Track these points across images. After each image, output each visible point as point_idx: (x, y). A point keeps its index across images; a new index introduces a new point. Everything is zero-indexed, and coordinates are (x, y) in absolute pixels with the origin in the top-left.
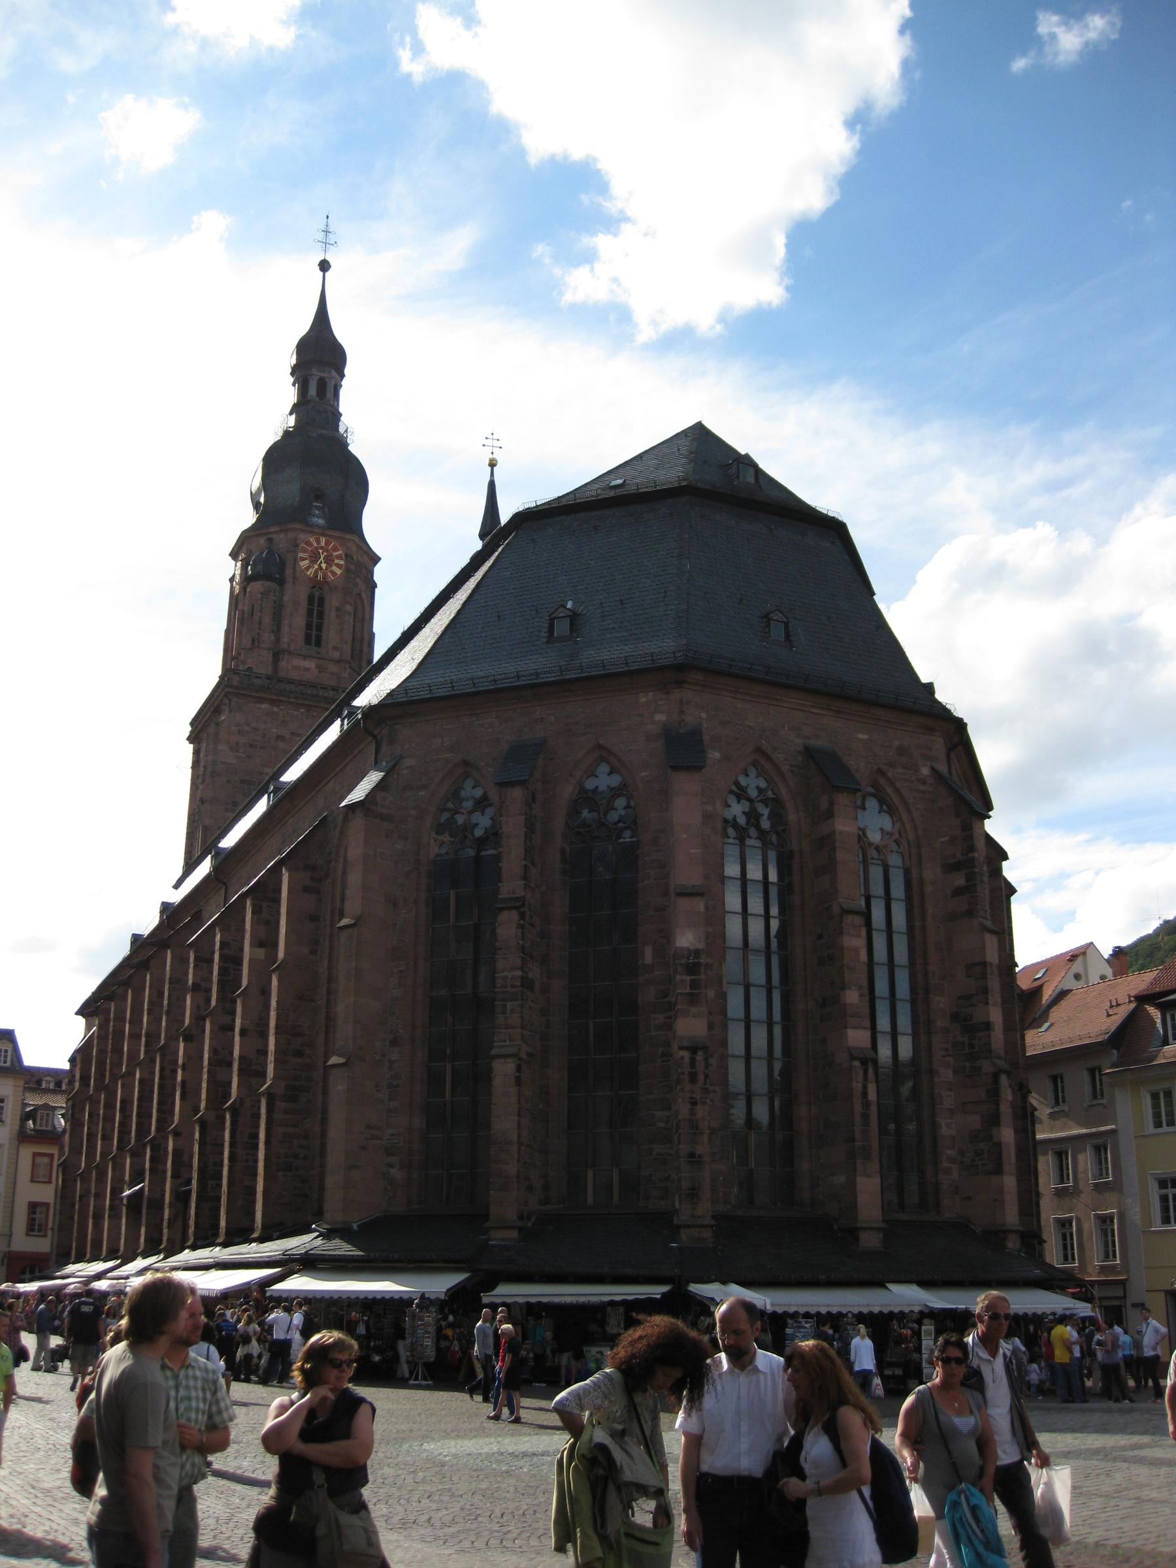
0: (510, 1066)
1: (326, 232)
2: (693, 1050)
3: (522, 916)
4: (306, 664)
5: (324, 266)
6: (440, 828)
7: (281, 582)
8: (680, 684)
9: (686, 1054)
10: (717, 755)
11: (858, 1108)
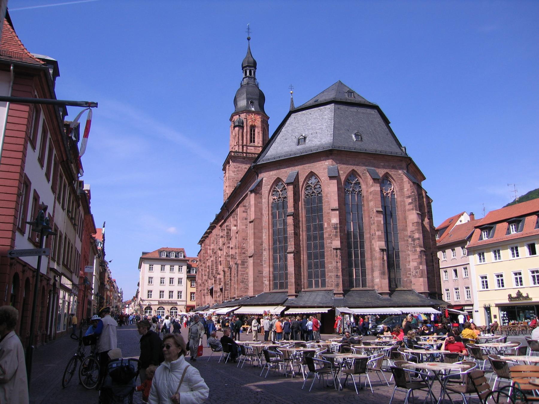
0: (292, 255)
1: (249, 29)
4: (251, 148)
5: (249, 39)
6: (273, 195)
7: (243, 127)
8: (331, 154)
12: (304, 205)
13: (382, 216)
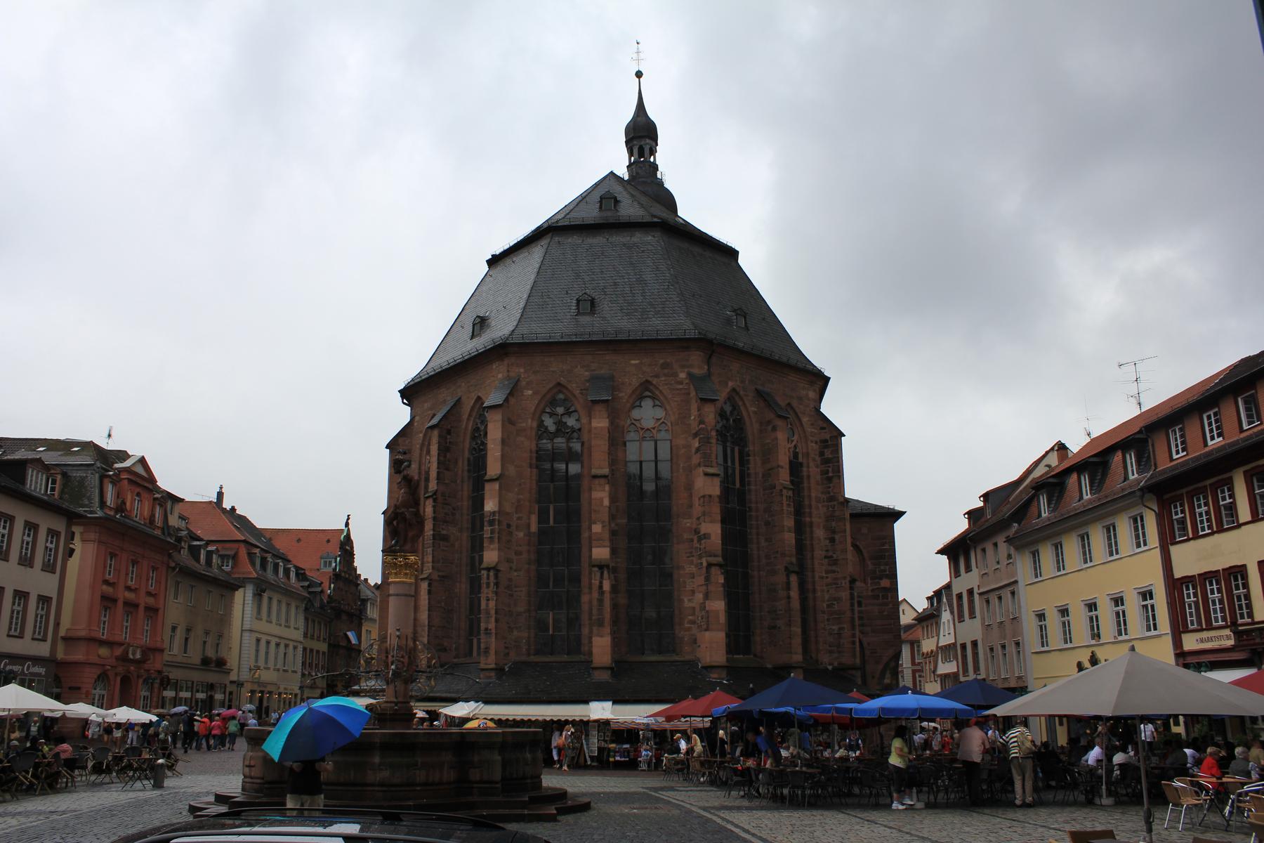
2: (488, 569)
3: (435, 501)
5: (639, 75)
8: (506, 354)
9: (484, 573)
10: (530, 392)
11: (595, 595)
12: (469, 471)
13: (607, 488)
